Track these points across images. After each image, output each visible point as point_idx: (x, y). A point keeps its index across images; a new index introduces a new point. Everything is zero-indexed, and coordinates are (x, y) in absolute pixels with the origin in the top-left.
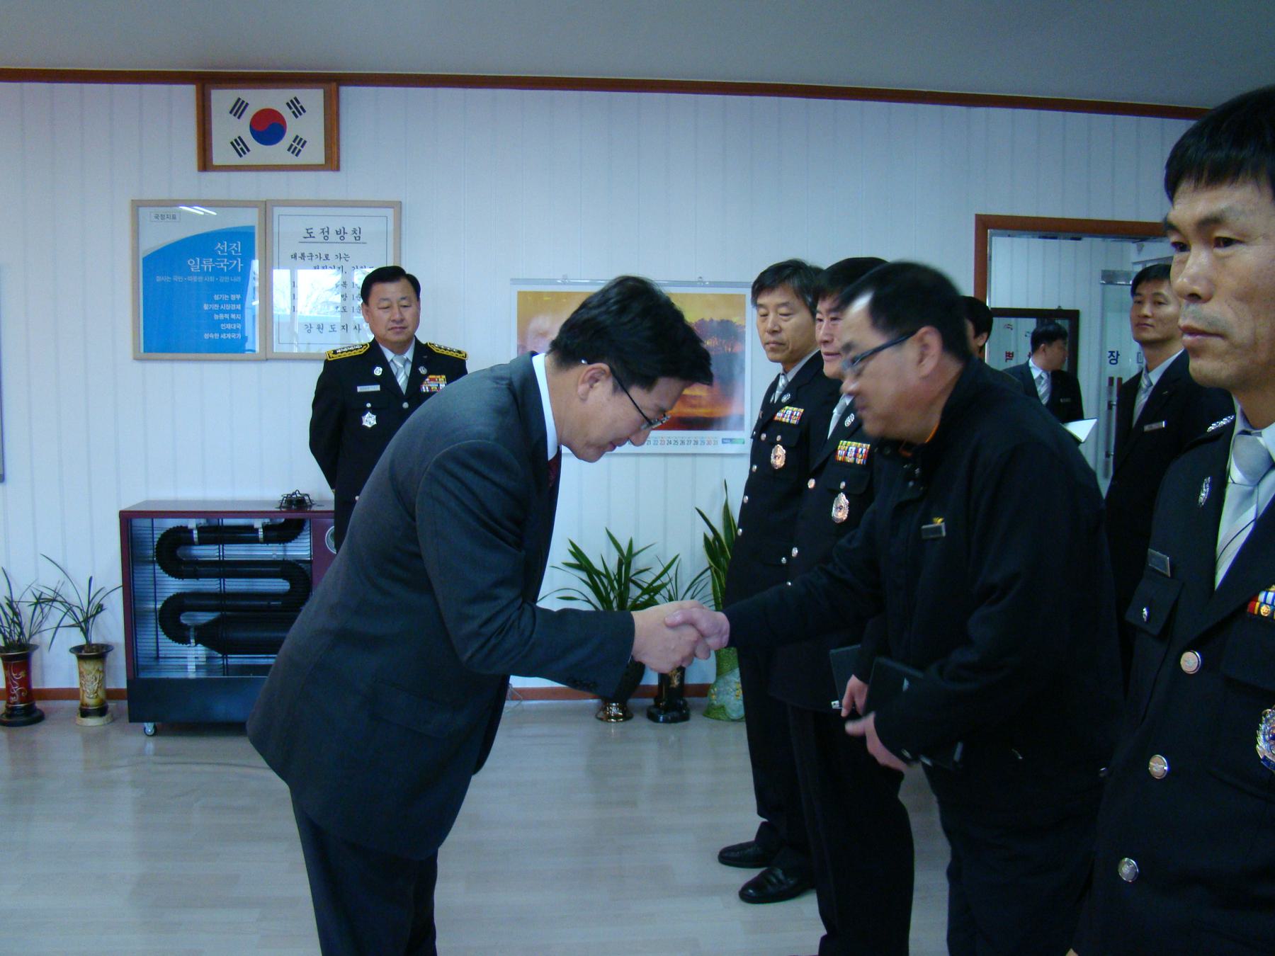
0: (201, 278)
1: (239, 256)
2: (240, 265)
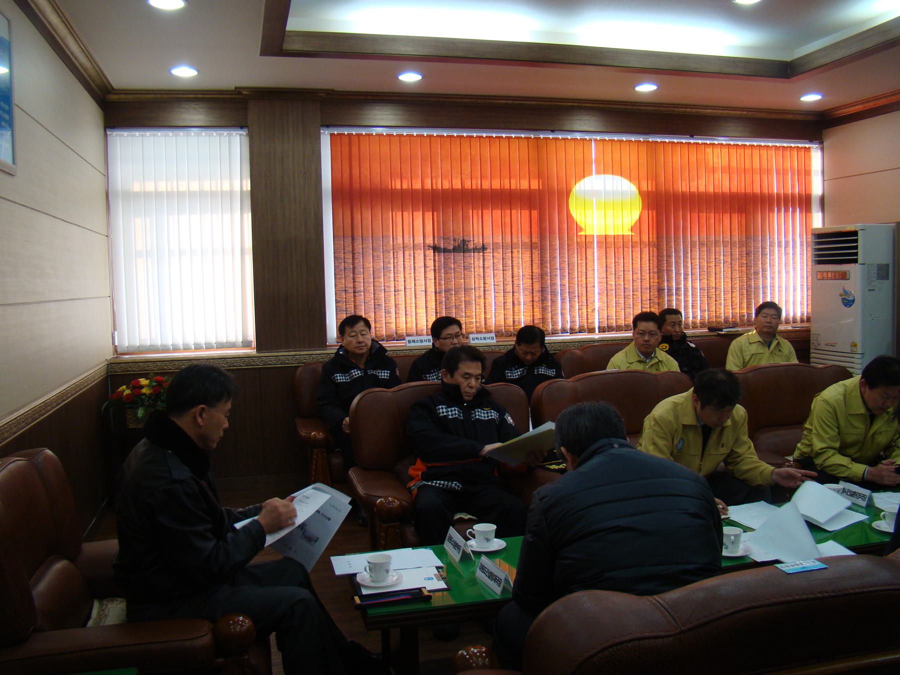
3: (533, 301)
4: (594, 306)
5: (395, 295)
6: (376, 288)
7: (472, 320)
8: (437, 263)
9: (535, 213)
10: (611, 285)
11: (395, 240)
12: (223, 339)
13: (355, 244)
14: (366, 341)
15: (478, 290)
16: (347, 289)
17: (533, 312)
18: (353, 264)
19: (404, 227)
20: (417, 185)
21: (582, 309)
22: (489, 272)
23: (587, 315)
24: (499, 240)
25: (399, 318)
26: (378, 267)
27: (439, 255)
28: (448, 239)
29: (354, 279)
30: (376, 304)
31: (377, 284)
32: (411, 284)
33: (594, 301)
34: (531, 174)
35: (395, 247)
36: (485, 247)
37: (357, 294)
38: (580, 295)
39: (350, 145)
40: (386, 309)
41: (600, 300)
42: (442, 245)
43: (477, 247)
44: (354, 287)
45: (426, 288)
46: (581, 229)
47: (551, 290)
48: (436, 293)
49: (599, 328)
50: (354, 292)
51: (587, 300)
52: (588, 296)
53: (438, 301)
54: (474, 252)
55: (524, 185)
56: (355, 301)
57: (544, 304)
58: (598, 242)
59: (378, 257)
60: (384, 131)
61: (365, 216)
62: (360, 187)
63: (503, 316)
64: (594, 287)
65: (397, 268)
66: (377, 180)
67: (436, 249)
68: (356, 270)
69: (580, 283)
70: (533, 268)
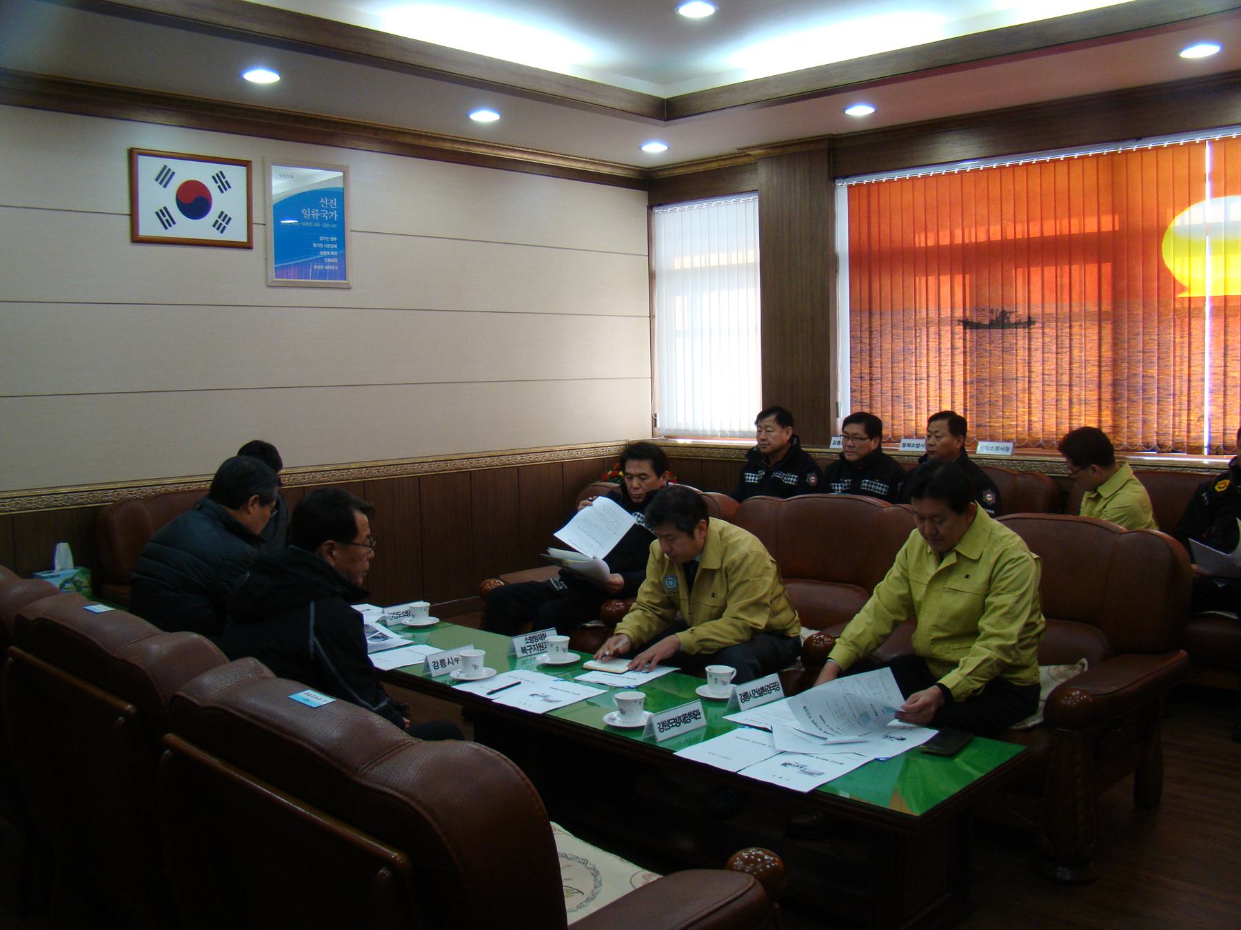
0: (311, 224)
1: (335, 209)
2: (336, 216)
3: (1100, 399)
4: (1202, 411)
5: (916, 385)
6: (895, 375)
7: (1013, 423)
8: (968, 343)
9: (1107, 268)
10: (1234, 377)
11: (918, 313)
12: (727, 428)
13: (873, 320)
14: (770, 438)
15: (1021, 382)
16: (863, 375)
17: (1100, 415)
18: (870, 344)
19: (929, 296)
20: (945, 241)
21: (1180, 415)
22: (1037, 356)
23: (1189, 425)
24: (1050, 308)
25: (921, 414)
26: (898, 348)
27: (971, 333)
28: (984, 310)
29: (871, 363)
30: (895, 395)
31: (896, 370)
32: (934, 372)
33: (1203, 404)
34: (1102, 208)
35: (917, 323)
36: (1032, 320)
37: (874, 382)
38: (1177, 393)
39: (869, 196)
40: (906, 402)
41: (1212, 402)
42: (975, 318)
43: (1022, 321)
44: (870, 374)
45: (952, 376)
46: (1183, 289)
47: (1128, 383)
48: (965, 383)
49: (1210, 446)
50: (871, 380)
51: (1189, 401)
52: (1192, 395)
53: (968, 394)
54: (1016, 328)
55: (1091, 226)
56: (871, 391)
57: (1118, 404)
58: (1213, 309)
59: (898, 336)
60: (968, 166)
61: (883, 284)
62: (880, 249)
63: (1055, 420)
64: (1203, 380)
65: (920, 350)
66: (897, 237)
67: (966, 324)
68: (874, 352)
69: (1178, 374)
70: (1103, 350)
